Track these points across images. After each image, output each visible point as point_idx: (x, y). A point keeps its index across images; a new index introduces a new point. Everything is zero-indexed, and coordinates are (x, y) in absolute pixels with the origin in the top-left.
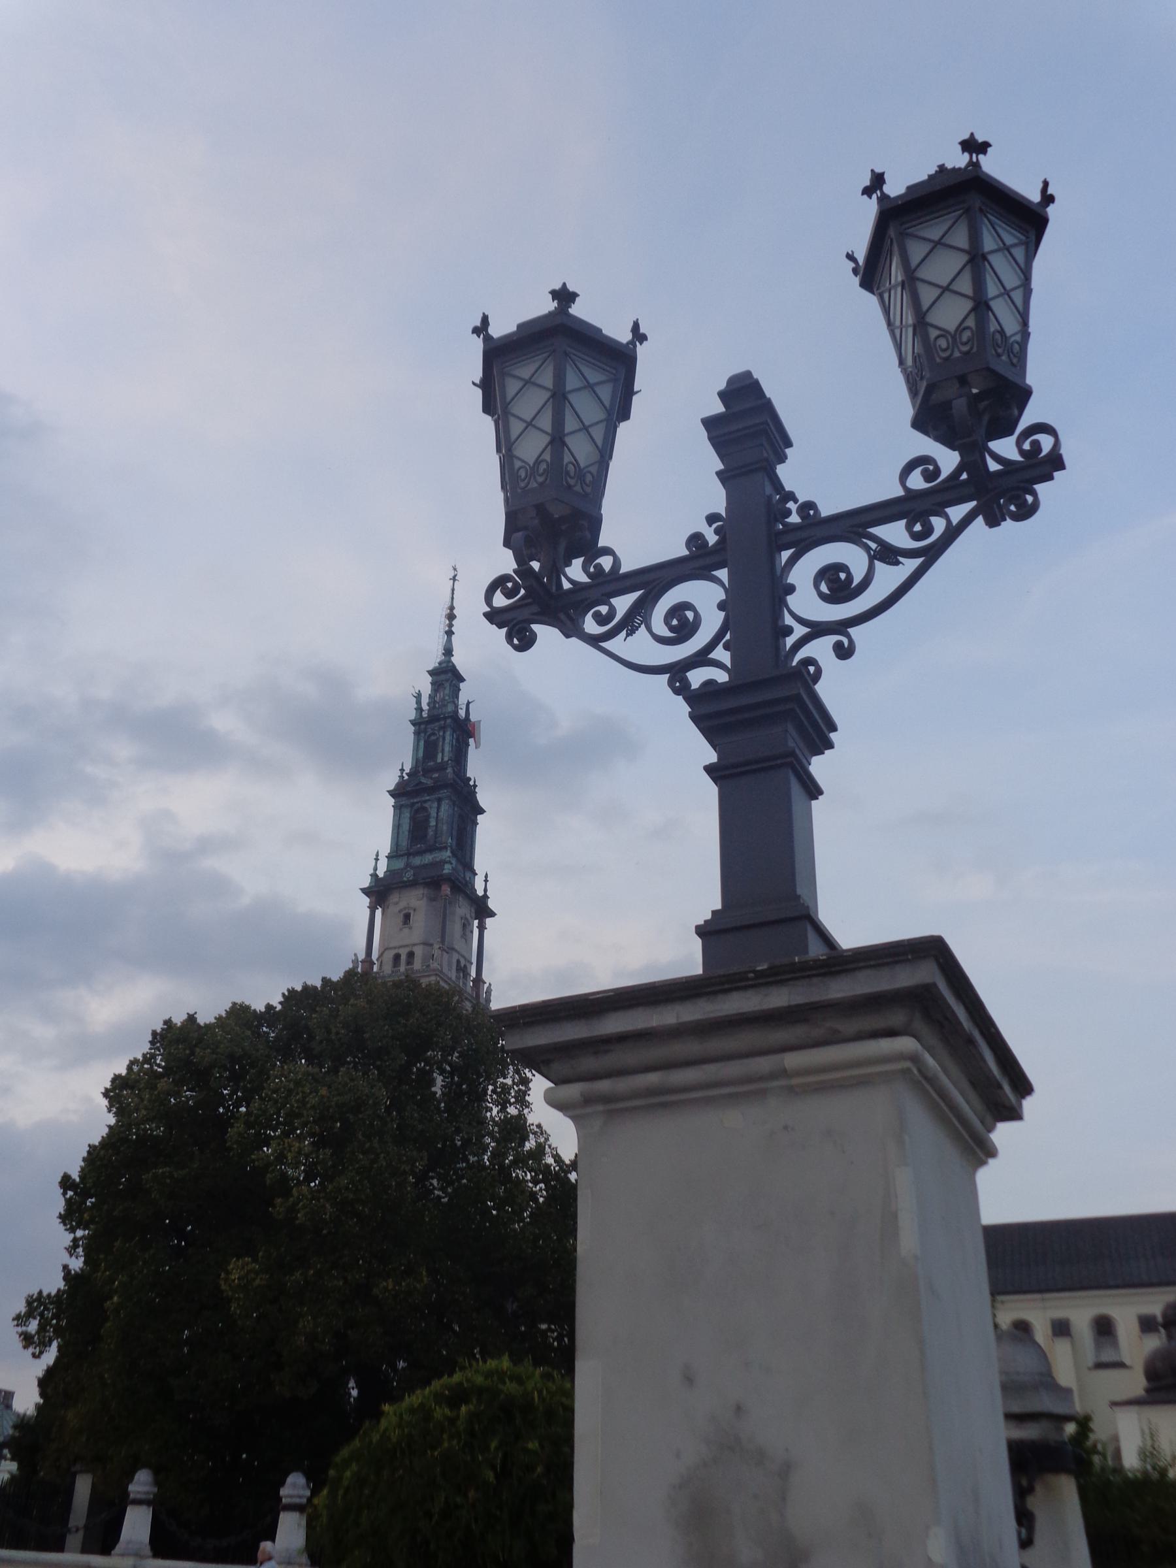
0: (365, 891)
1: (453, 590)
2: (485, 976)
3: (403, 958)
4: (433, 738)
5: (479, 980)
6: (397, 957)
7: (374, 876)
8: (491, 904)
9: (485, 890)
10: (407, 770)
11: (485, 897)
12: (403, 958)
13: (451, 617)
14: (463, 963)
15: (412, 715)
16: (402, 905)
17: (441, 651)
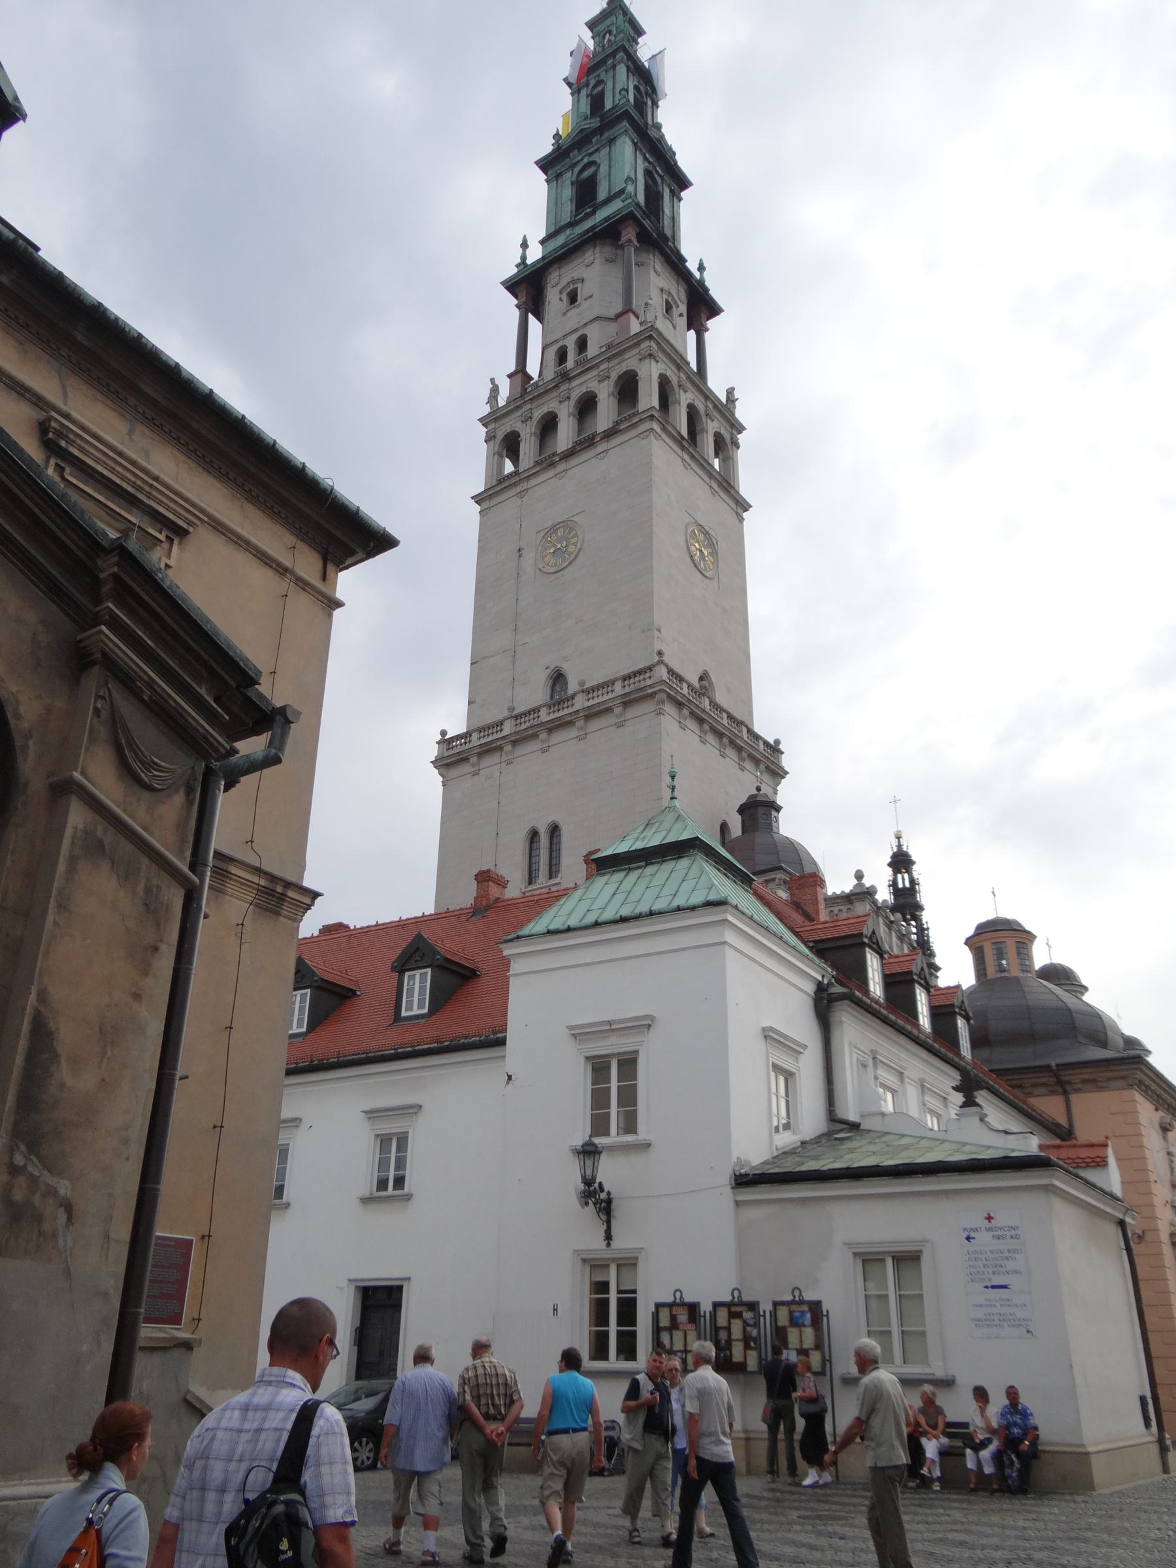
0: (512, 286)
4: (599, 88)
6: (562, 356)
16: (564, 282)
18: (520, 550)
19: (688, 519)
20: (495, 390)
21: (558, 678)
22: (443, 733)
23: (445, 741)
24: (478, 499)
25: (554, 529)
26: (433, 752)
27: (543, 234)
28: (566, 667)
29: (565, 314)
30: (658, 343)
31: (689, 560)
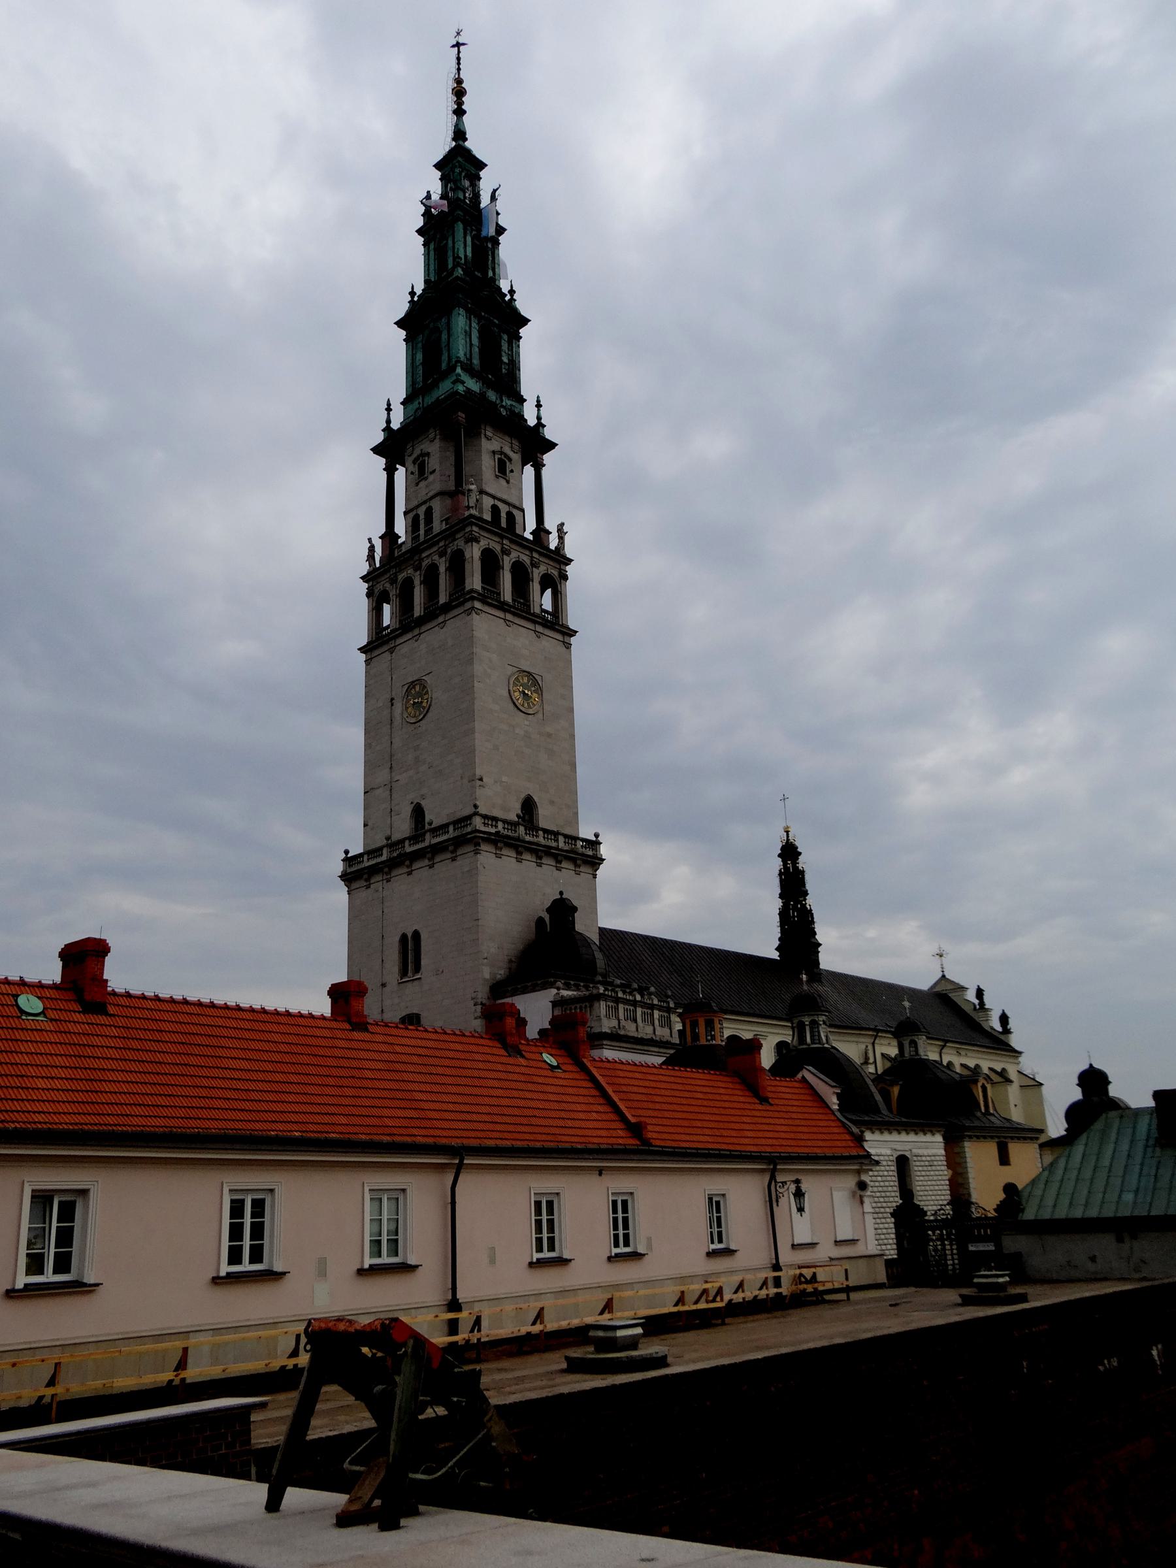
0: (377, 450)
1: (459, 59)
2: (550, 524)
3: (422, 517)
5: (541, 531)
7: (388, 429)
8: (549, 434)
9: (539, 418)
10: (419, 290)
11: (540, 425)
12: (422, 517)
13: (459, 93)
14: (504, 509)
15: (420, 222)
16: (417, 452)
17: (450, 134)
18: (392, 699)
19: (510, 670)
20: (372, 549)
21: (418, 812)
22: (347, 852)
23: (349, 860)
24: (362, 650)
25: (412, 684)
26: (339, 867)
27: (403, 395)
28: (423, 803)
29: (417, 484)
30: (477, 525)
31: (511, 706)
